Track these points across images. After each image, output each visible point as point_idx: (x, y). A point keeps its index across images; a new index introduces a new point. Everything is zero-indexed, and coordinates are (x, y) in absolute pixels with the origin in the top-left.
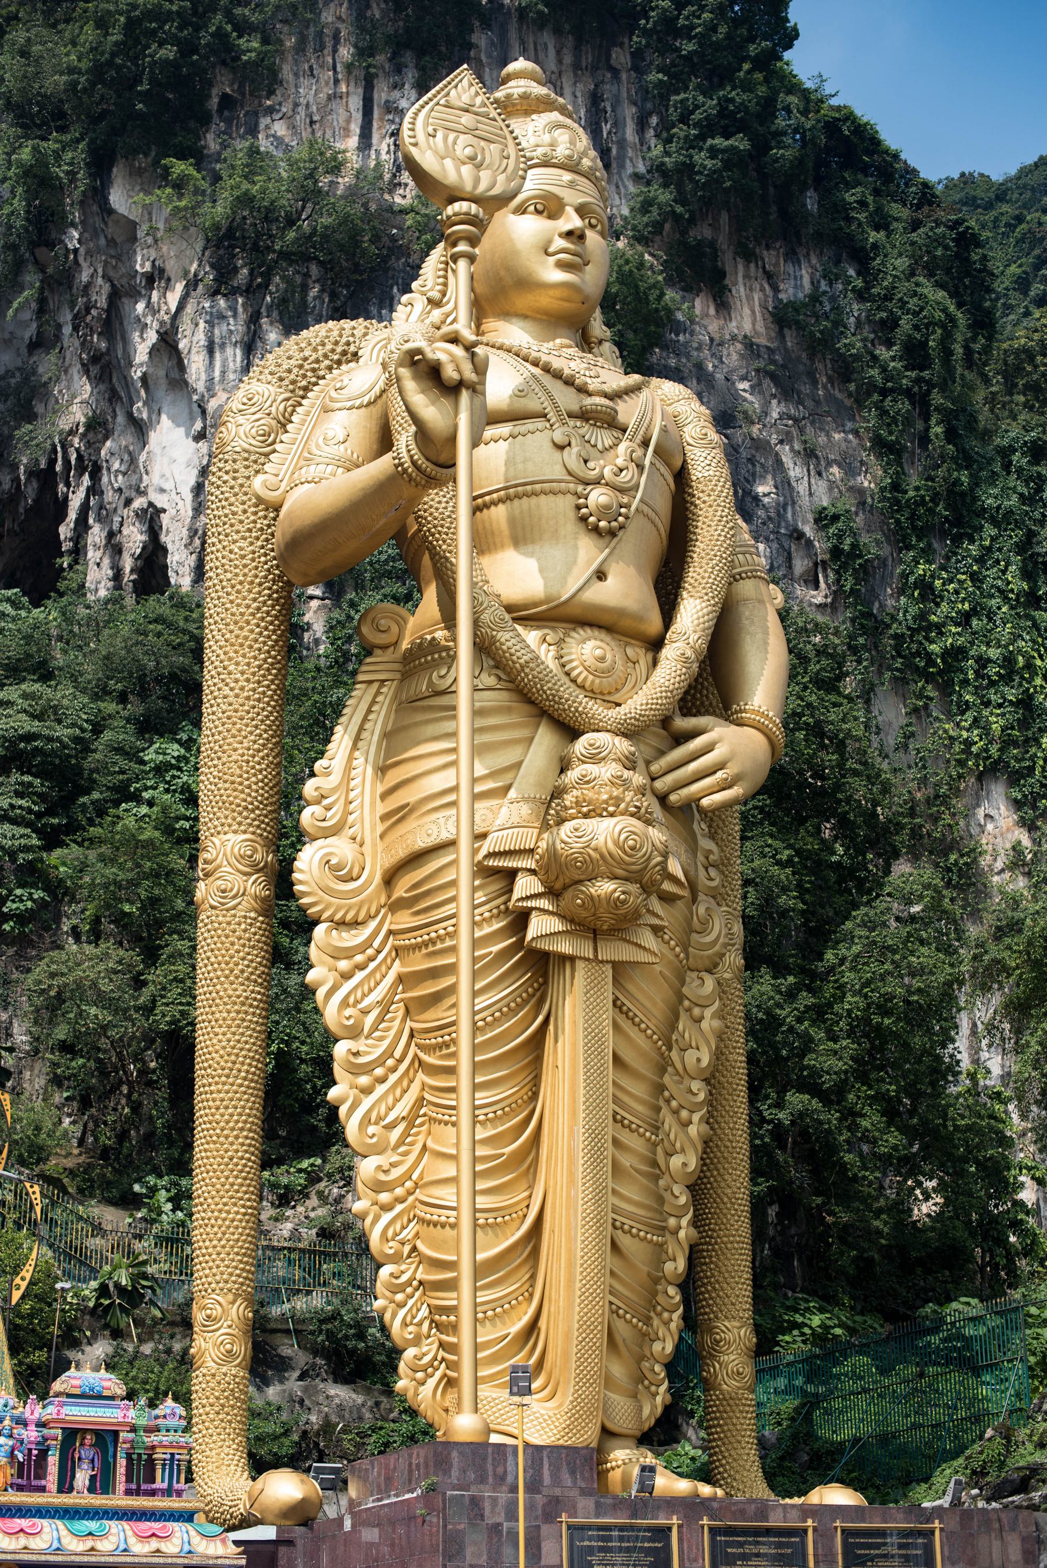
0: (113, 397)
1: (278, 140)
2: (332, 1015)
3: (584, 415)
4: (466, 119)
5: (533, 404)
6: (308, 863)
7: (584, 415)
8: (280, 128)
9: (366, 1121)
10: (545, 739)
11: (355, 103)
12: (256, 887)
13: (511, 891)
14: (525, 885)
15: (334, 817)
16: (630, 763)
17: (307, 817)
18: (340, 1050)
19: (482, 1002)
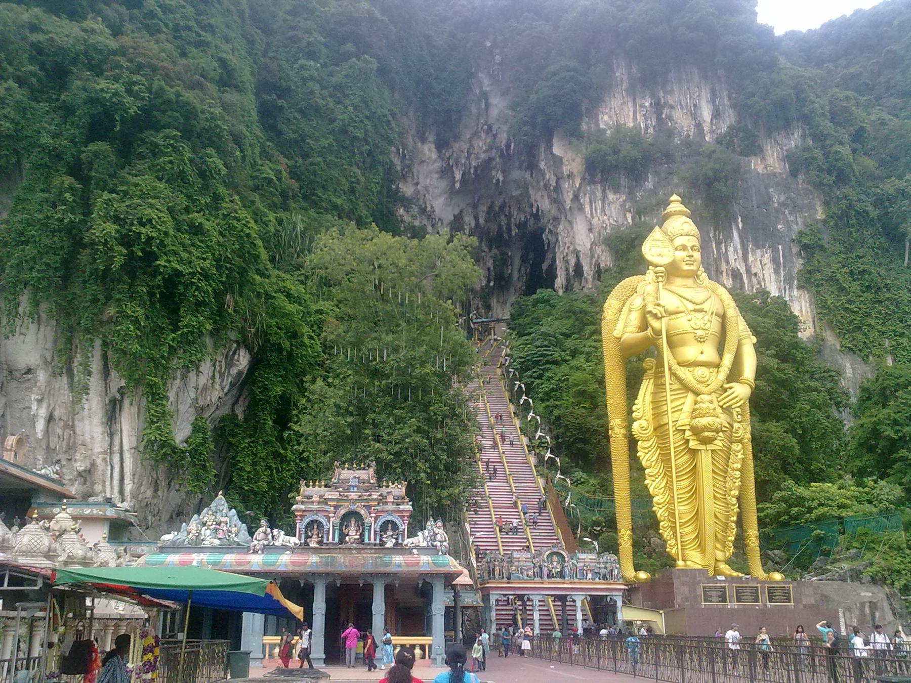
0: (559, 209)
1: (606, 123)
2: (644, 463)
3: (695, 311)
4: (659, 243)
5: (682, 309)
6: (636, 426)
7: (695, 311)
8: (606, 118)
9: (655, 488)
10: (691, 396)
11: (630, 104)
12: (623, 431)
13: (684, 433)
14: (688, 433)
15: (640, 415)
16: (711, 402)
17: (634, 415)
18: (647, 471)
19: (679, 461)
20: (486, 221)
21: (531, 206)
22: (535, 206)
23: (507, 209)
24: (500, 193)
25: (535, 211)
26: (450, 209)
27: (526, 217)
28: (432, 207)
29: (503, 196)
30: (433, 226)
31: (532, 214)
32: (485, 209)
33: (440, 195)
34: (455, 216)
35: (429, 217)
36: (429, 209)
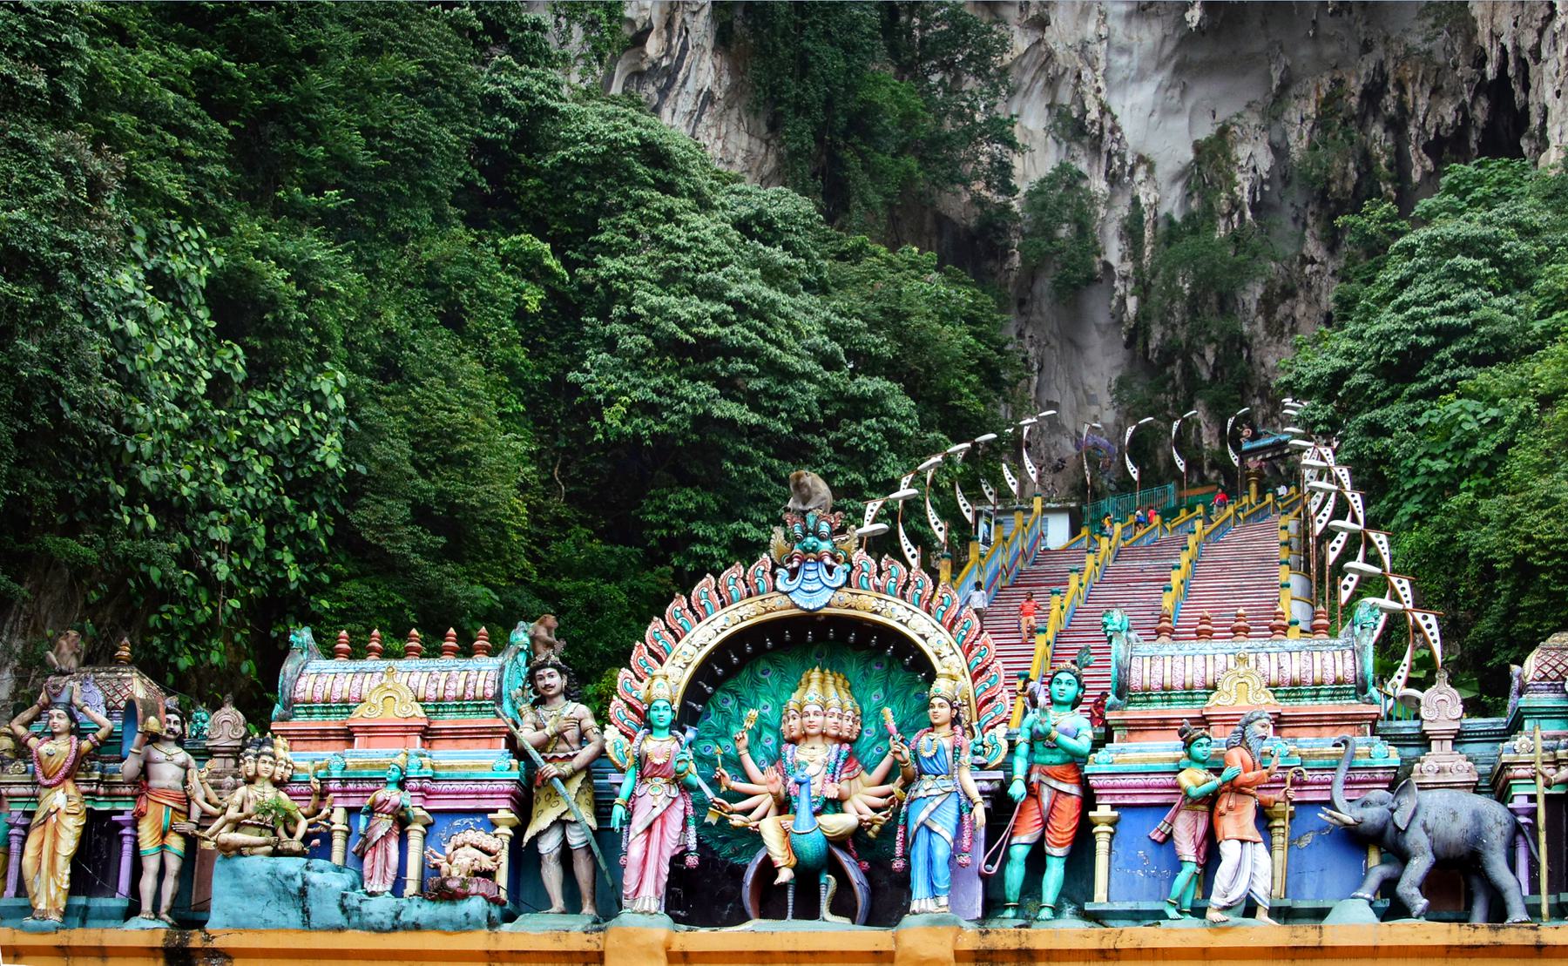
20: (1313, 147)
21: (1480, 60)
22: (1495, 54)
23: (1389, 102)
24: (1367, 47)
25: (1490, 70)
26: (1181, 123)
27: (1462, 108)
28: (1104, 110)
29: (1379, 52)
30: (1113, 179)
31: (1482, 88)
32: (1311, 110)
33: (1141, 76)
34: (1198, 148)
35: (1096, 146)
36: (1094, 114)
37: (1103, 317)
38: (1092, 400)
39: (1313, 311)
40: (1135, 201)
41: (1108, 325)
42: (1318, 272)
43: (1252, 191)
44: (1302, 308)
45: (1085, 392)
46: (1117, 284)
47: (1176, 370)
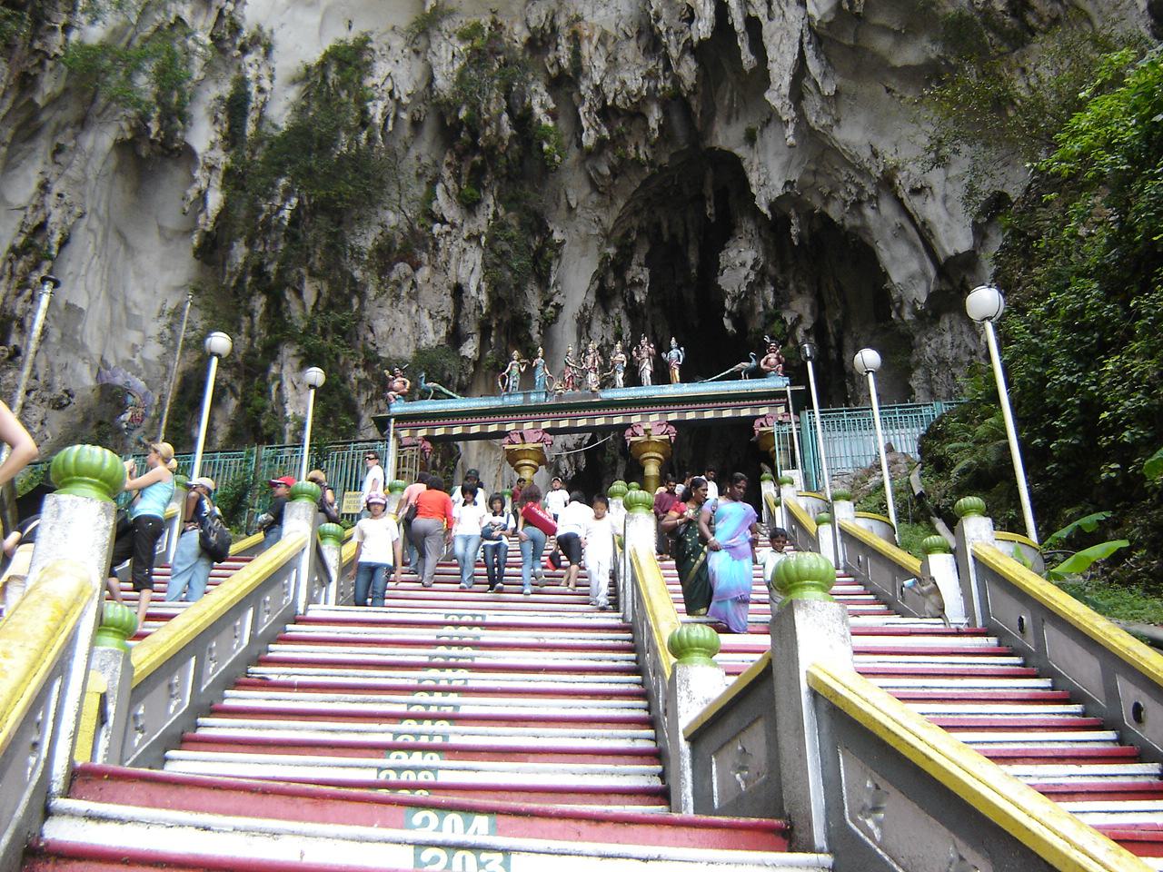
21: (690, 16)
23: (564, 53)
25: (703, 28)
26: (312, 19)
30: (217, 40)
37: (172, 218)
38: (133, 322)
39: (439, 278)
40: (241, 83)
41: (176, 232)
42: (448, 233)
43: (386, 117)
44: (424, 272)
45: (126, 308)
46: (198, 174)
47: (259, 303)
